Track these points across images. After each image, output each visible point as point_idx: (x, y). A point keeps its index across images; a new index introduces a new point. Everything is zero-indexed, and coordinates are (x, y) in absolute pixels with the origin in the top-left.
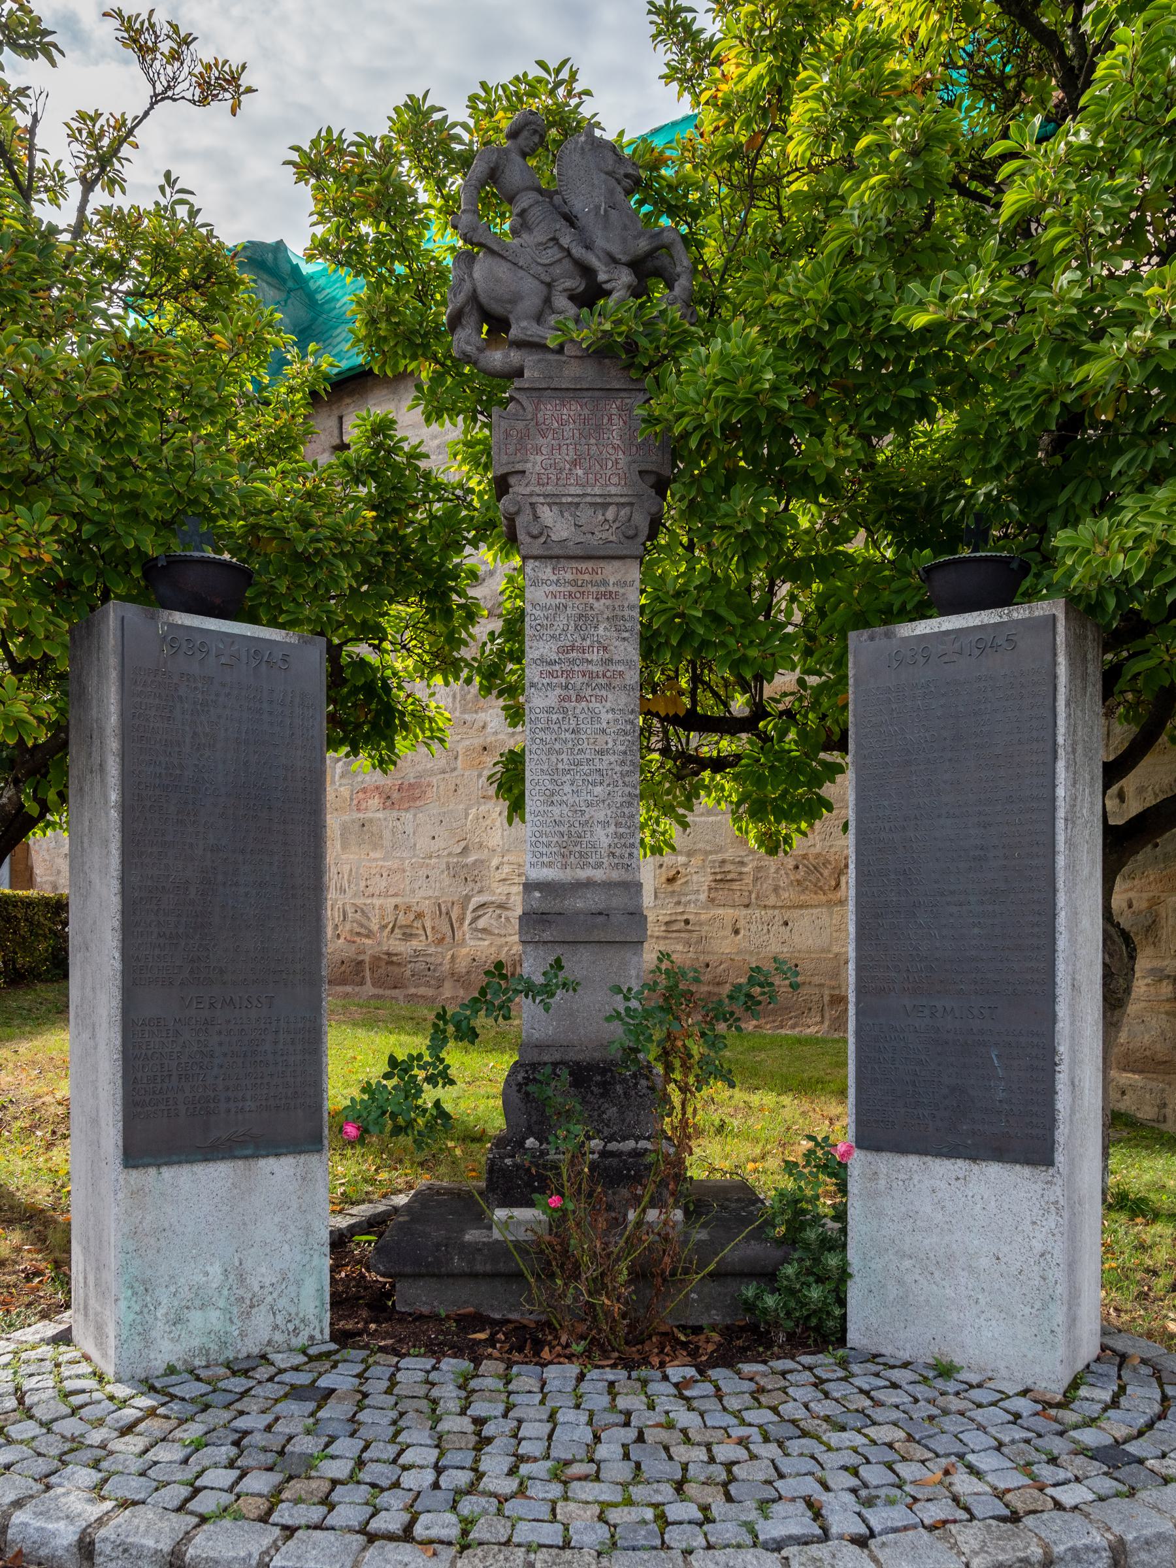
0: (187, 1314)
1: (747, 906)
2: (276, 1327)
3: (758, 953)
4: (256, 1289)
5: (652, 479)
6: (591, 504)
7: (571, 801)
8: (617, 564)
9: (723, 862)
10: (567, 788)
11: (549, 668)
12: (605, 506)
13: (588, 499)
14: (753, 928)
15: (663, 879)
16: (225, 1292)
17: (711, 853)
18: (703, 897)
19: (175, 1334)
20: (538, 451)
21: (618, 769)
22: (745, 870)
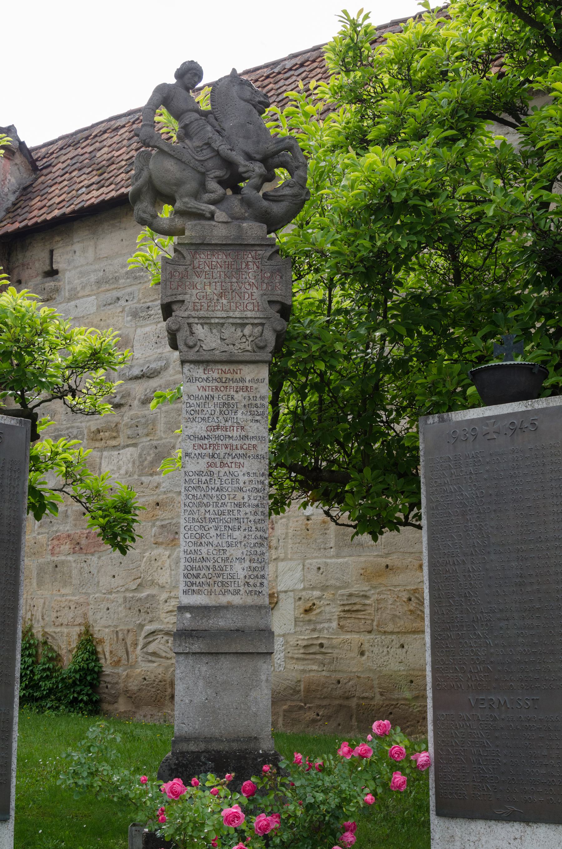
1: (370, 632)
3: (380, 672)
5: (278, 307)
7: (215, 542)
8: (252, 367)
9: (351, 595)
10: (213, 532)
11: (200, 442)
12: (243, 325)
13: (231, 321)
14: (376, 650)
15: (302, 610)
17: (340, 588)
18: (334, 624)
20: (194, 286)
21: (252, 518)
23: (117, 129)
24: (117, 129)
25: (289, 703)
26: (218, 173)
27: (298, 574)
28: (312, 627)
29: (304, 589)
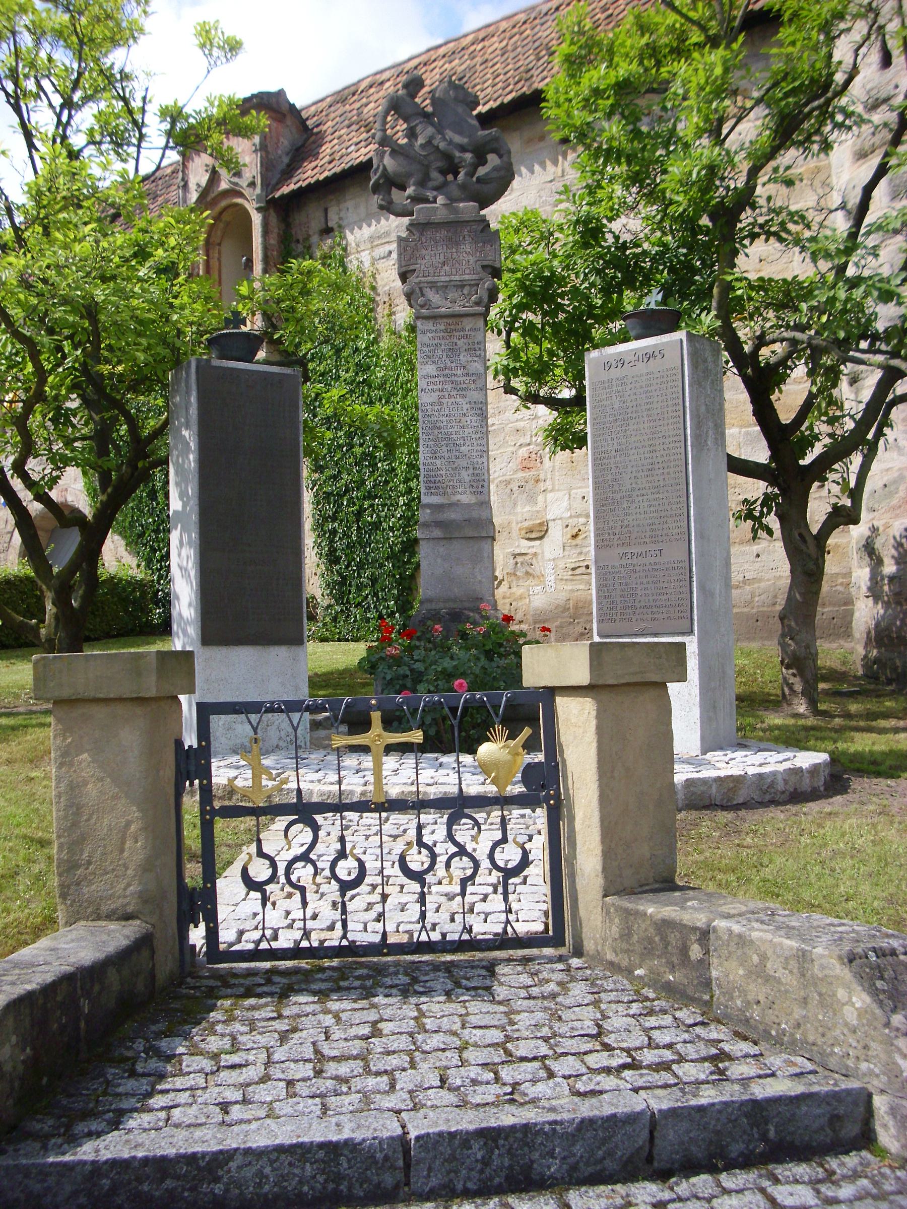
5: (490, 270)
8: (470, 319)
10: (444, 449)
12: (463, 286)
15: (569, 536)
20: (423, 258)
21: (474, 436)
23: (382, 83)
24: (382, 83)
25: (560, 620)
26: (439, 164)
27: (565, 504)
28: (578, 551)
29: (571, 517)
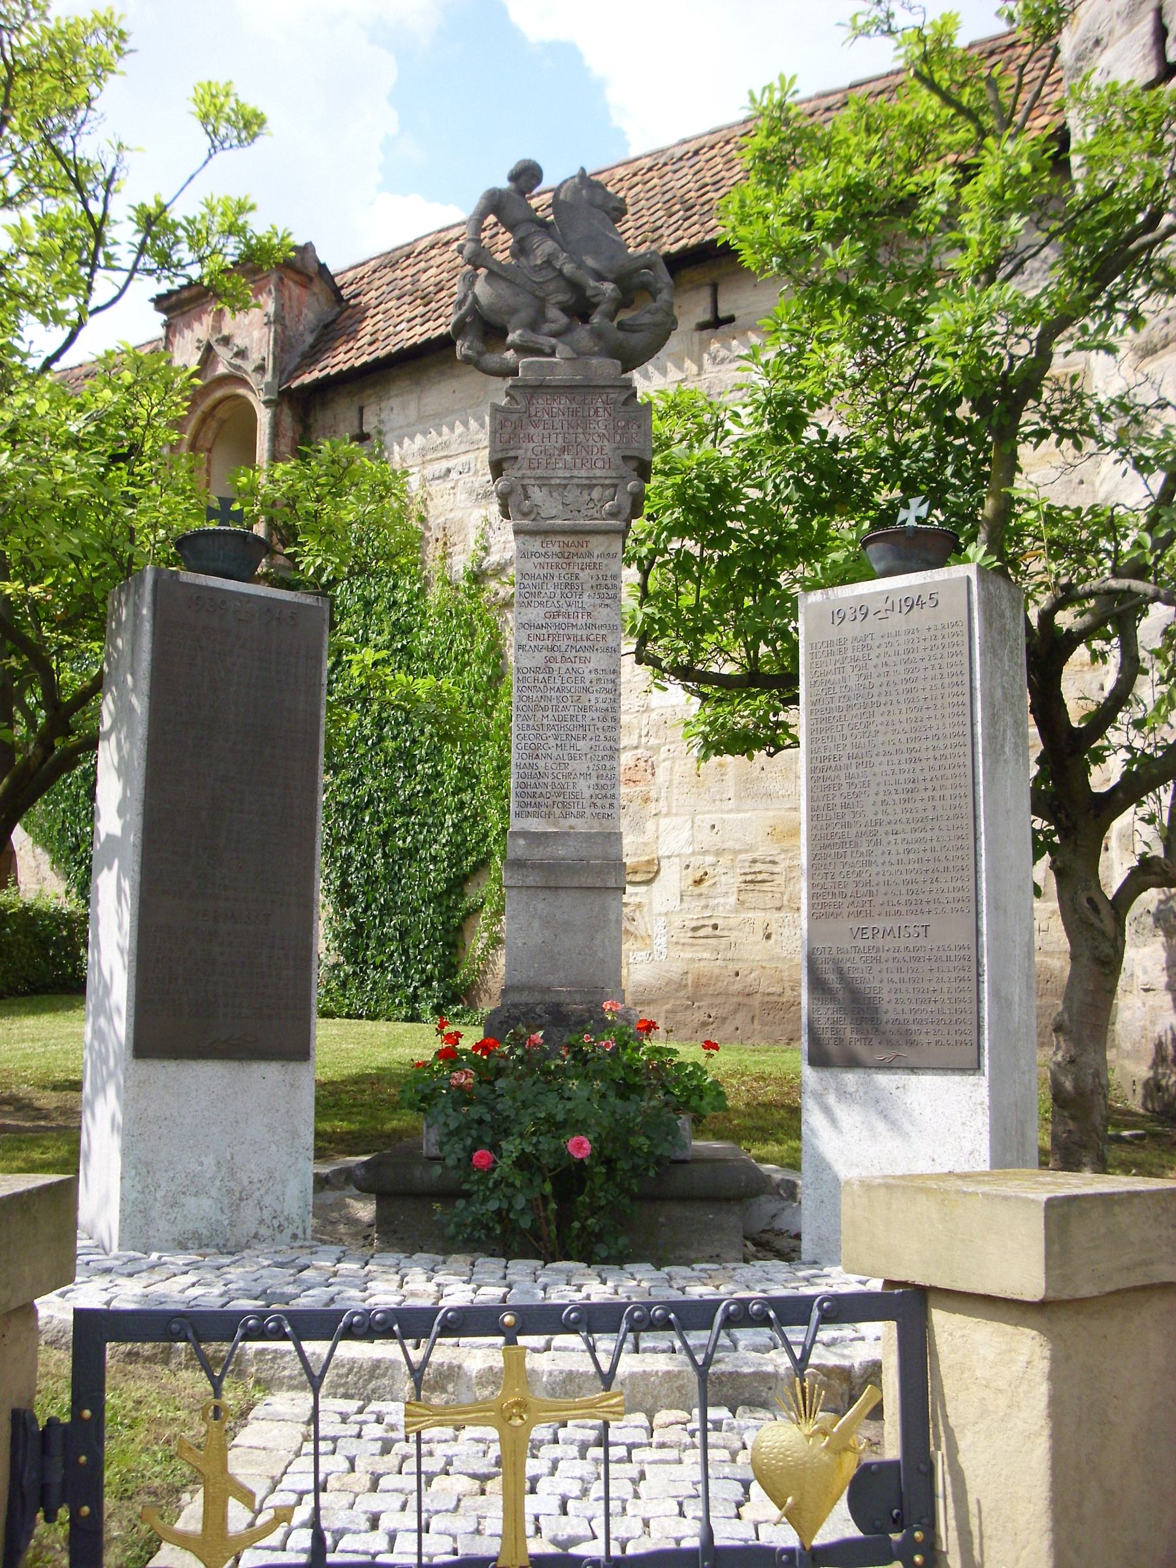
0: (182, 1199)
1: (779, 909)
2: (262, 1222)
3: (791, 960)
4: (246, 1183)
5: (634, 464)
6: (578, 485)
7: (555, 755)
8: (601, 538)
9: (754, 861)
10: (552, 742)
11: (537, 632)
12: (591, 487)
13: (576, 481)
14: (786, 932)
15: (690, 881)
16: (218, 1183)
17: (740, 852)
18: (732, 900)
19: (172, 1216)
21: (600, 725)
22: (776, 869)
23: (447, 243)
24: (447, 243)
25: (672, 1002)
26: (561, 297)
27: (686, 835)
28: (703, 902)
29: (693, 853)
